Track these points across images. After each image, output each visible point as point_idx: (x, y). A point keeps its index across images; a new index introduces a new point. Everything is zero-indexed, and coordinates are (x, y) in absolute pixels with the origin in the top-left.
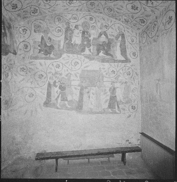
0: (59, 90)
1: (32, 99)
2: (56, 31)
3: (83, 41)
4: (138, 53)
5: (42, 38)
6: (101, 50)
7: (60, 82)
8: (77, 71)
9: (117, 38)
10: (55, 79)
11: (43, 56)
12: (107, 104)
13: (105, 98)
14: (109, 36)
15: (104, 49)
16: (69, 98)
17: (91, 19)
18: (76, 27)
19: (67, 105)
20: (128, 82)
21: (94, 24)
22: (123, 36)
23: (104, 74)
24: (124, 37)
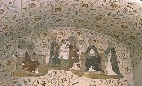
2: (42, 46)
3: (70, 56)
4: (130, 68)
5: (27, 53)
6: (90, 65)
9: (107, 52)
11: (27, 72)
14: (98, 50)
15: (94, 65)
17: (79, 34)
18: (63, 41)
21: (82, 39)
22: (113, 51)
24: (115, 52)
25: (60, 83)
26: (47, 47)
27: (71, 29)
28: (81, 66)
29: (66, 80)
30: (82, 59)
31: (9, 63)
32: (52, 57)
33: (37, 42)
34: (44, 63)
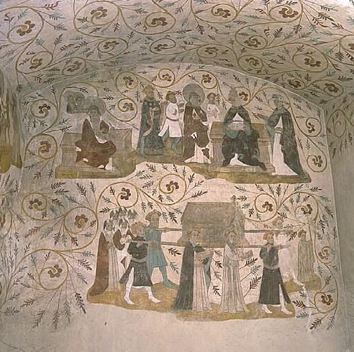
0: (129, 258)
1: (59, 281)
3: (187, 131)
4: (325, 158)
5: (86, 125)
6: (234, 151)
7: (131, 235)
8: (176, 206)
9: (272, 122)
10: (117, 227)
11: (88, 169)
12: (257, 291)
13: (248, 276)
14: (251, 117)
15: (241, 151)
16: (156, 276)
17: (207, 79)
18: (171, 97)
19: (151, 297)
20: (308, 234)
21: (214, 91)
23: (245, 211)
24: (290, 121)
25: (164, 193)
26: (132, 109)
27: (189, 68)
28: (211, 153)
29: (177, 188)
30: (214, 137)
31: (46, 146)
32: (146, 134)
33: (109, 98)
34: (126, 147)
